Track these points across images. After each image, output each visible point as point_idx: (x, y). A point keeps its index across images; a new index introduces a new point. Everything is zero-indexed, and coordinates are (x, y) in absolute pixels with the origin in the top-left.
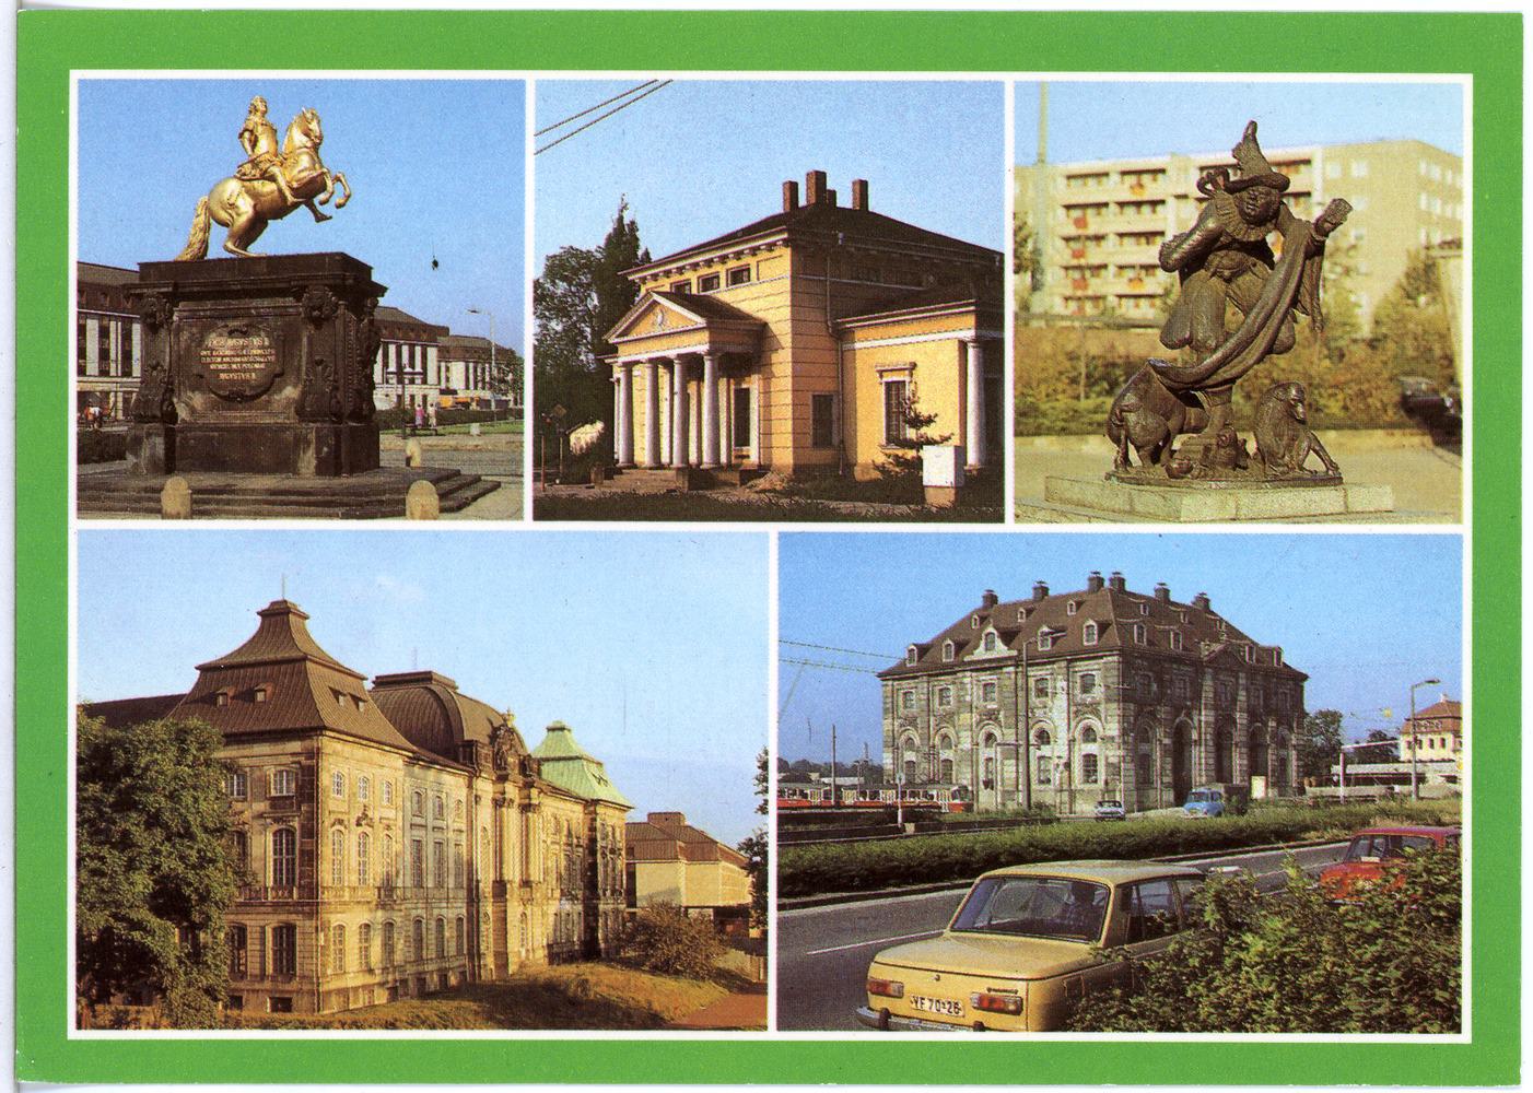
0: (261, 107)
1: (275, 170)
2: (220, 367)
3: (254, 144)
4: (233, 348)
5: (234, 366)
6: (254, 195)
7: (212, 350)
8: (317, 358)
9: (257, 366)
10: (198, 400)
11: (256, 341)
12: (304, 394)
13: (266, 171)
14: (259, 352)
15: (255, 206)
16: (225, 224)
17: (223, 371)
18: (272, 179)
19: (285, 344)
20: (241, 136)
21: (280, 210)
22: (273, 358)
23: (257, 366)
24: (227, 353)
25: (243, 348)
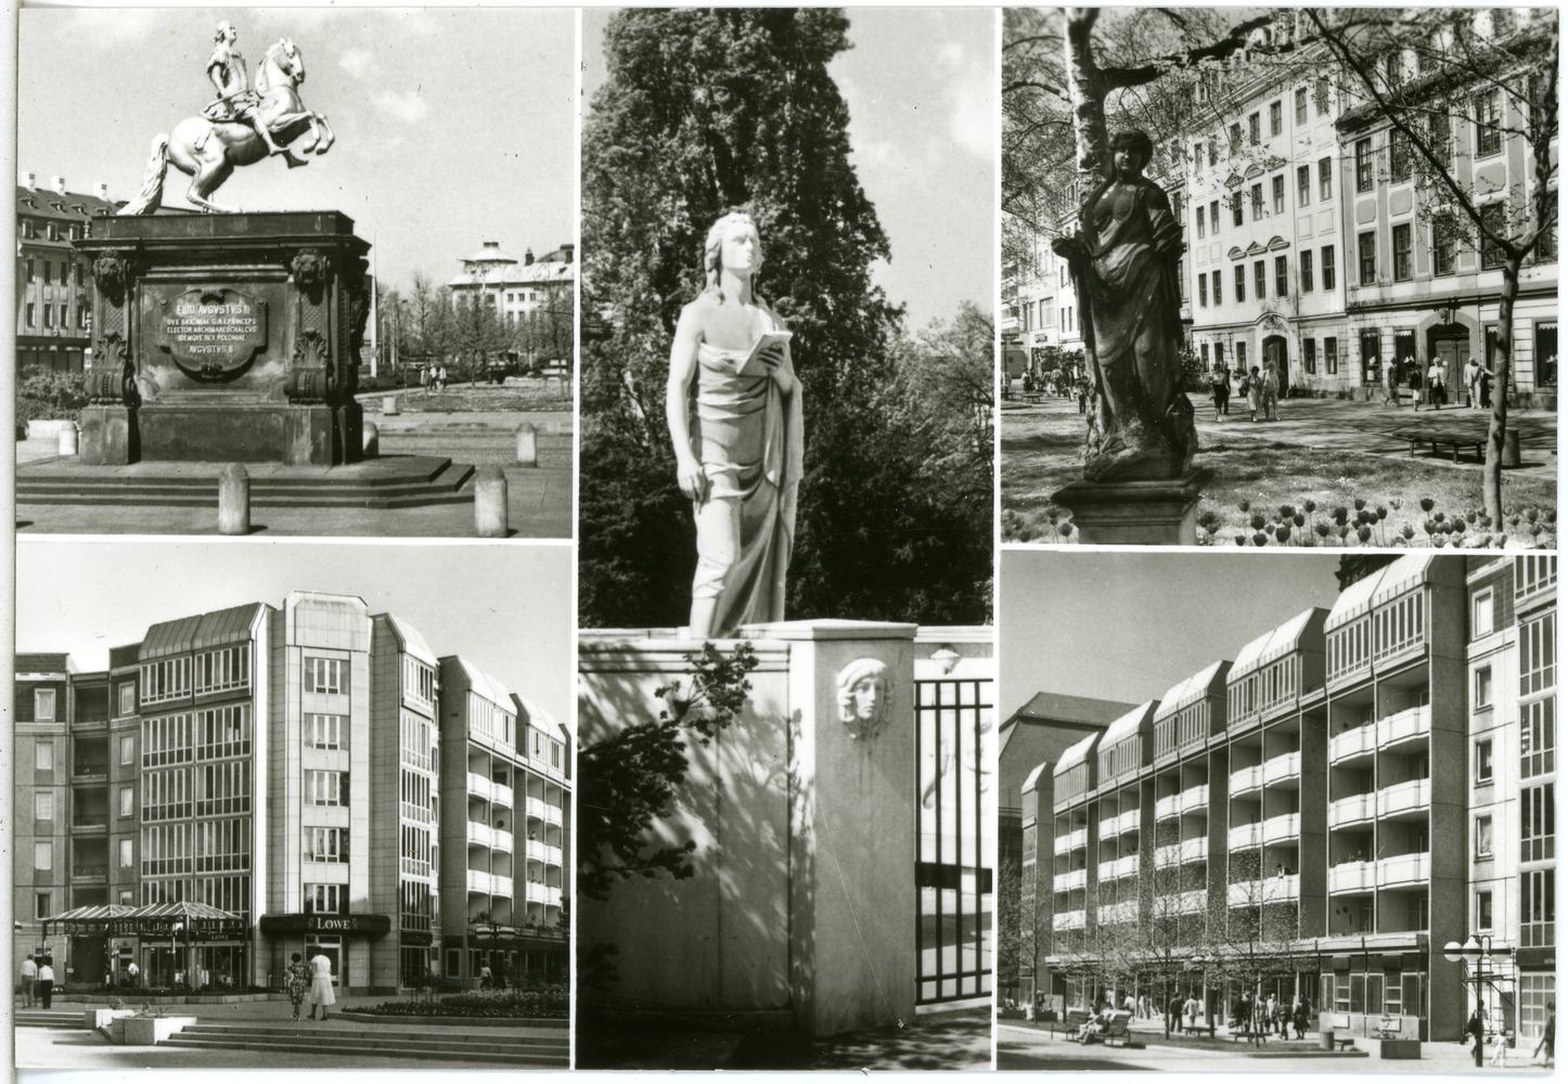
0: (229, 35)
1: (251, 112)
3: (226, 80)
4: (206, 316)
5: (207, 338)
7: (180, 319)
8: (310, 329)
10: (161, 375)
13: (243, 113)
14: (239, 321)
15: (226, 152)
16: (190, 172)
18: (250, 122)
19: (267, 314)
20: (210, 70)
21: (252, 152)
24: (199, 322)
25: (218, 315)
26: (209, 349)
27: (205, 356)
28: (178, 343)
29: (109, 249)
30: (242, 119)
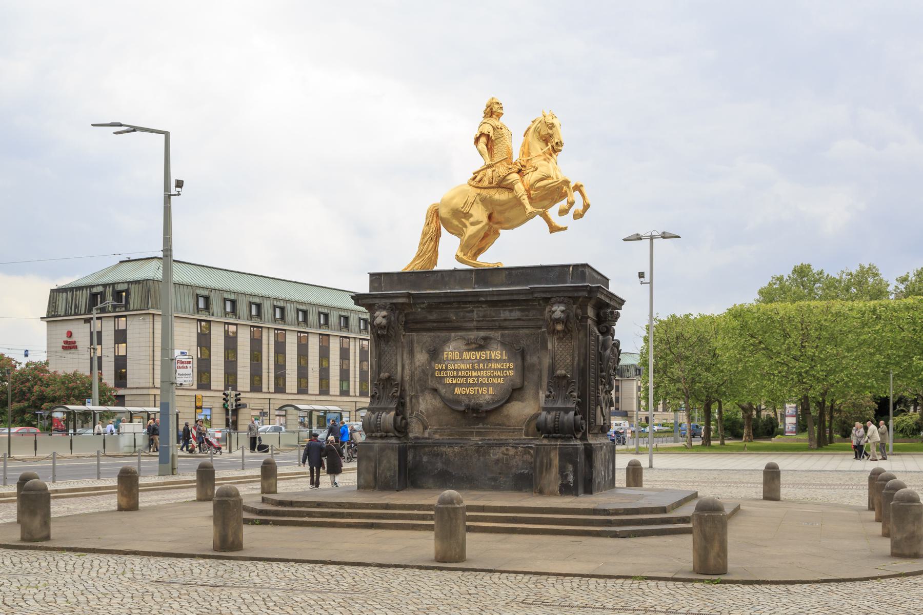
2: (455, 382)
5: (470, 381)
9: (494, 380)
11: (497, 353)
13: (504, 178)
14: (498, 366)
17: (461, 385)
22: (511, 373)
23: (494, 380)
24: (463, 366)
26: (471, 391)
27: (468, 396)
28: (445, 385)
29: (383, 301)
30: (503, 184)
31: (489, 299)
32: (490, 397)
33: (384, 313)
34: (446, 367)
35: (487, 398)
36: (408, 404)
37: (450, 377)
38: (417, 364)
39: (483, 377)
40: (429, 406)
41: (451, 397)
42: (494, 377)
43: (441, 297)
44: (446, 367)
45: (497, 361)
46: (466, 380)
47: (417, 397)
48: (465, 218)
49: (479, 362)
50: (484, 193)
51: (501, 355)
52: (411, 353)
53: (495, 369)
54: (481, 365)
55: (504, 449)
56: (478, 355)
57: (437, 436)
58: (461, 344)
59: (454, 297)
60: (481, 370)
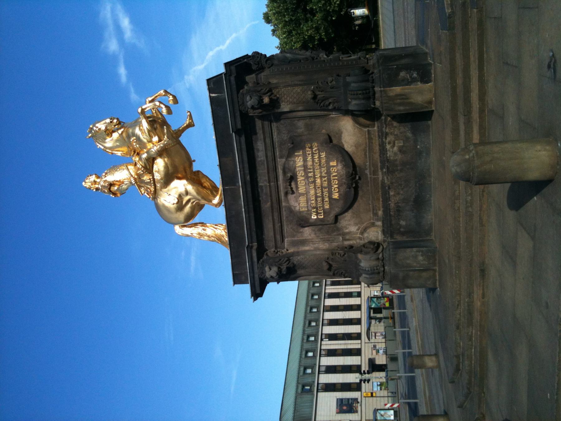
2: (327, 199)
4: (307, 185)
5: (325, 184)
6: (168, 179)
9: (323, 161)
11: (299, 162)
12: (347, 112)
14: (309, 158)
23: (323, 161)
24: (312, 192)
27: (340, 185)
28: (331, 208)
29: (256, 271)
31: (247, 171)
32: (339, 164)
33: (267, 269)
34: (314, 208)
35: (340, 167)
36: (351, 242)
37: (323, 204)
38: (313, 235)
39: (321, 173)
40: (352, 222)
41: (342, 202)
42: (320, 161)
43: (249, 217)
44: (314, 208)
45: (305, 161)
46: (325, 188)
47: (344, 234)
48: (182, 202)
49: (307, 177)
50: (158, 185)
51: (299, 156)
52: (303, 242)
53: (313, 161)
54: (310, 175)
55: (388, 147)
56: (300, 178)
57: (380, 213)
58: (291, 197)
59: (248, 205)
60: (314, 175)
